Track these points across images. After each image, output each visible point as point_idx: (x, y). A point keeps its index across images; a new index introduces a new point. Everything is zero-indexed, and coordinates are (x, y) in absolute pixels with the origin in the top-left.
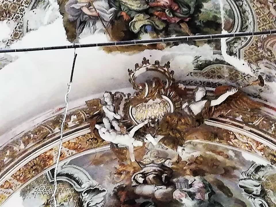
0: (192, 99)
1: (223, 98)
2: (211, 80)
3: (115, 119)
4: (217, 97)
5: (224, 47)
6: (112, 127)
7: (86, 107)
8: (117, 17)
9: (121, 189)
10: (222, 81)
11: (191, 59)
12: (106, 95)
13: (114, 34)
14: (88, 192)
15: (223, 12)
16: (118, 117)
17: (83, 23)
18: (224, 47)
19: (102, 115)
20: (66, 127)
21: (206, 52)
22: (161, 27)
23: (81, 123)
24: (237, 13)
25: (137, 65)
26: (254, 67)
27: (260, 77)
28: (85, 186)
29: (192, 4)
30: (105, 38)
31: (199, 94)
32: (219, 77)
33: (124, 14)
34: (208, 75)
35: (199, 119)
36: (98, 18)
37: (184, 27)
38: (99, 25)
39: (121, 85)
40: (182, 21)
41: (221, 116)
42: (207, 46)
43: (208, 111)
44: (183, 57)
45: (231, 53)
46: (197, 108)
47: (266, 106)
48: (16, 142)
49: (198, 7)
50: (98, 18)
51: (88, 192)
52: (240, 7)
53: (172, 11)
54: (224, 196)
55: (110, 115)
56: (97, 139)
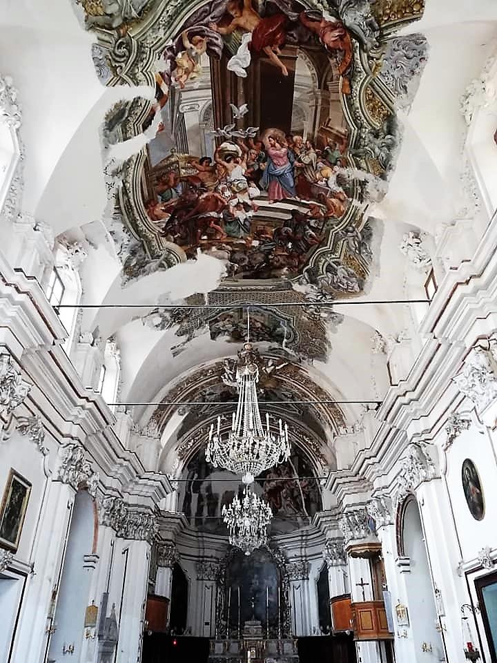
0: (267, 365)
1: (282, 366)
5: (284, 345)
7: (215, 365)
8: (235, 330)
11: (267, 346)
13: (233, 337)
14: (208, 395)
15: (285, 333)
17: (220, 333)
18: (284, 345)
19: (224, 371)
20: (206, 375)
21: (275, 345)
24: (292, 334)
28: (207, 392)
29: (272, 328)
30: (228, 338)
34: (274, 353)
37: (267, 336)
38: (226, 333)
39: (230, 354)
41: (281, 373)
43: (274, 371)
44: (264, 346)
45: (286, 347)
46: (269, 370)
49: (275, 329)
50: (225, 331)
51: (208, 395)
53: (263, 330)
54: (272, 395)
55: (229, 372)
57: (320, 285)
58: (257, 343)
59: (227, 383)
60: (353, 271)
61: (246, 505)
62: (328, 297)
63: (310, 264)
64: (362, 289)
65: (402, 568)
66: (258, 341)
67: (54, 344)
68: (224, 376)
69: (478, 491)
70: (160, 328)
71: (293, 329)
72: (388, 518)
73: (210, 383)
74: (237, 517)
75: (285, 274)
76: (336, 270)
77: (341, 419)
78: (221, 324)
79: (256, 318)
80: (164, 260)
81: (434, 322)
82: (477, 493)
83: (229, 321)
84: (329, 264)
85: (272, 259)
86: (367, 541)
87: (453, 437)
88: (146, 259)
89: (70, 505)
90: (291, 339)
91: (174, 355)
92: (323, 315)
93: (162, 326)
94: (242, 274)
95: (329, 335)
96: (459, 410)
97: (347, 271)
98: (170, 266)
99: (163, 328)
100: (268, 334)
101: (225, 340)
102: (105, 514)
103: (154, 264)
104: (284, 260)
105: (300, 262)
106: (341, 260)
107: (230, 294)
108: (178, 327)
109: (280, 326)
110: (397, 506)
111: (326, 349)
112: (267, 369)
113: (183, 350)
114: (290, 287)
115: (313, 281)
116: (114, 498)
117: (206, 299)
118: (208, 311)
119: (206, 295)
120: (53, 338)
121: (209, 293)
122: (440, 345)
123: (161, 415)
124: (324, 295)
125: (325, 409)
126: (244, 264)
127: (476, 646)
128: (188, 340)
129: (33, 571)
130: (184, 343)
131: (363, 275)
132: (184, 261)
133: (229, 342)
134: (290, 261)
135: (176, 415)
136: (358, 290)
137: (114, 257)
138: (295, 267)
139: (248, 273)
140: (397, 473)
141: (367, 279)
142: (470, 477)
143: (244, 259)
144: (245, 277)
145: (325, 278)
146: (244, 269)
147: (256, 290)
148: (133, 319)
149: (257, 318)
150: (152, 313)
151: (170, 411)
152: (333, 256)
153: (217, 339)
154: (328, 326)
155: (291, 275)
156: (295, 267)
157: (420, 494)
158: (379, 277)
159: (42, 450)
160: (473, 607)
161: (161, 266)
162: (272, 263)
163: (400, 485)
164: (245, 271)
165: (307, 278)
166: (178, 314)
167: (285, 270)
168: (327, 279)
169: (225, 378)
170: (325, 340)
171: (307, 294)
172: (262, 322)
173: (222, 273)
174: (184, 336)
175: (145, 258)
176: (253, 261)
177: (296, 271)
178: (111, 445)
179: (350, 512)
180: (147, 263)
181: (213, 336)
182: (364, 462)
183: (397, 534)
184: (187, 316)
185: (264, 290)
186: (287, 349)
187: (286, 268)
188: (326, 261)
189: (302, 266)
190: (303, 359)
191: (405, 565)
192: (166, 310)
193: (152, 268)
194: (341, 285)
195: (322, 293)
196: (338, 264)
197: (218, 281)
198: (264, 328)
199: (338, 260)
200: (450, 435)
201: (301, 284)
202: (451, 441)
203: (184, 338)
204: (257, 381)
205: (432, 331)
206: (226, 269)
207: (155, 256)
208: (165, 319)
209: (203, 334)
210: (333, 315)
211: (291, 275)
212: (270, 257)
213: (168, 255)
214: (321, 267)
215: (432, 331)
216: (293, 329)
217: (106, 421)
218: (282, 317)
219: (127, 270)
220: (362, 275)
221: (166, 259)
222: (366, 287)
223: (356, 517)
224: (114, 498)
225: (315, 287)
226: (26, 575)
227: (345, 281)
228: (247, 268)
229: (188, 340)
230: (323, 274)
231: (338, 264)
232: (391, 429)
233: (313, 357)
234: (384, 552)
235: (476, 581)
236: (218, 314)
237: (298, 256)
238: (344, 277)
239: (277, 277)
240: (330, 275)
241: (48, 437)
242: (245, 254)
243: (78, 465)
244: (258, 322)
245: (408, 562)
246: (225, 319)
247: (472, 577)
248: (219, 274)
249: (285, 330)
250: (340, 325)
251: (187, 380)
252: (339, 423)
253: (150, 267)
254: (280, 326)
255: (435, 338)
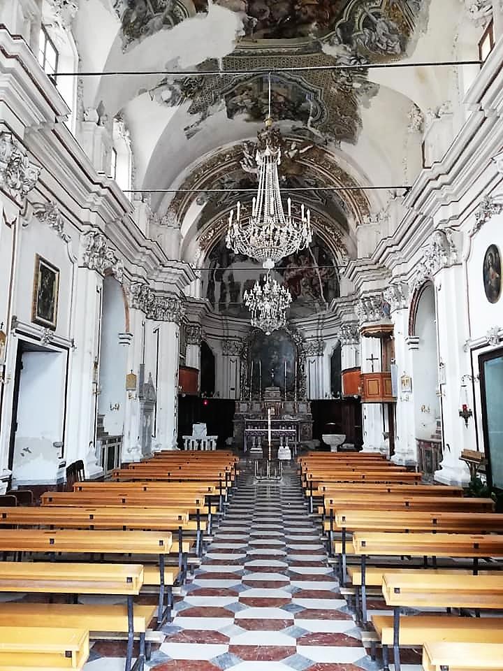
2: (299, 136)
3: (250, 159)
4: (302, 149)
5: (309, 124)
6: (248, 162)
7: (233, 149)
9: (243, 180)
10: (304, 137)
12: (245, 144)
15: (312, 108)
16: (252, 157)
17: (237, 110)
18: (309, 124)
19: (243, 156)
20: (224, 160)
21: (299, 124)
22: (277, 111)
23: (231, 158)
24: (319, 108)
25: (263, 130)
26: (323, 134)
27: (326, 141)
28: (226, 180)
30: (246, 116)
31: (293, 146)
32: (304, 135)
33: (259, 105)
35: (293, 160)
36: (245, 107)
37: (290, 113)
38: (245, 110)
40: (289, 110)
42: (300, 122)
43: (298, 155)
44: (286, 125)
45: (312, 126)
46: (291, 154)
47: (326, 152)
48: (199, 170)
49: (299, 104)
50: (243, 107)
51: (227, 183)
52: (321, 108)
53: (285, 105)
54: (294, 183)
55: (248, 156)
56: (240, 167)
57: (355, 45)
58: (278, 122)
59: (246, 169)
60: (395, 25)
61: (266, 290)
62: (363, 61)
63: (344, 16)
64: (403, 49)
65: (411, 346)
66: (279, 119)
67: (56, 122)
68: (243, 161)
69: (498, 276)
70: (170, 104)
71: (320, 104)
72: (403, 302)
73: (228, 170)
74: (258, 301)
75: (313, 31)
76: (374, 25)
77: (365, 207)
78: (238, 98)
79: (278, 91)
80: (169, 14)
81: (483, 90)
82: (497, 278)
83: (247, 95)
84: (367, 17)
85: (299, 10)
86: (381, 323)
87: (482, 222)
88: (148, 14)
89: (99, 289)
90: (318, 117)
91: (189, 136)
92: (356, 85)
93: (172, 102)
94: (263, 32)
95: (362, 111)
96: (493, 194)
97: (387, 25)
98: (176, 22)
99: (173, 105)
100: (293, 111)
101: (242, 119)
102: (134, 299)
103: (157, 20)
104: (314, 12)
105: (332, 14)
106: (382, 11)
107: (248, 59)
108: (189, 103)
109: (305, 101)
110: (414, 291)
111: (356, 128)
112: (290, 153)
113: (196, 131)
114: (319, 50)
115: (347, 41)
116: (140, 284)
117: (221, 67)
118: (224, 80)
119: (220, 62)
120: (54, 114)
121: (224, 58)
122: (485, 118)
123: (179, 204)
124: (359, 59)
125: (350, 197)
126: (264, 17)
127: (470, 407)
128: (203, 119)
129: (73, 346)
130: (198, 123)
131: (408, 31)
132: (193, 16)
133: (247, 121)
134: (320, 12)
135: (194, 203)
136: (399, 52)
137: (109, 10)
138: (327, 21)
139: (269, 31)
140: (417, 260)
141: (411, 34)
142: (492, 263)
143: (265, 11)
144: (266, 36)
145: (362, 36)
146: (264, 25)
147: (280, 53)
148: (139, 94)
149: (280, 90)
150: (162, 85)
151: (188, 200)
152: (374, 5)
153: (235, 117)
154: (360, 99)
155: (321, 33)
156: (327, 21)
157: (438, 281)
158: (425, 33)
159: (63, 237)
160: (473, 376)
161: (166, 22)
162: (299, 17)
163: (419, 271)
164: (265, 27)
165: (339, 36)
166: (190, 86)
167: (313, 26)
168: (363, 37)
169: (244, 164)
170: (356, 117)
171: (340, 57)
172: (285, 95)
173: (238, 32)
174: (198, 113)
175: (146, 12)
176: (276, 15)
177: (326, 26)
178: (131, 234)
179: (366, 298)
180: (150, 18)
181: (230, 115)
182: (385, 251)
183: (410, 316)
184: (200, 89)
185: (287, 53)
186: (313, 130)
187: (315, 23)
188: (365, 11)
189: (333, 20)
190: (330, 140)
191: (414, 343)
192: (176, 81)
193: (155, 25)
194: (380, 45)
195: (356, 55)
196: (378, 15)
197: (233, 41)
198: (287, 103)
199: (378, 10)
200: (479, 220)
201: (332, 44)
202: (479, 227)
203: (198, 116)
204: (279, 163)
205: (479, 102)
206: (243, 26)
207: (159, 9)
208: (174, 93)
209: (218, 112)
210: (367, 86)
211: (321, 33)
212: (297, 7)
213: (174, 7)
214: (357, 20)
215: (479, 102)
216: (320, 104)
217: (124, 210)
218: (308, 89)
219: (127, 29)
220: (405, 30)
221: (172, 13)
222: (409, 48)
223: (372, 302)
224: (140, 284)
225: (348, 48)
226: (68, 349)
227: (384, 40)
228: (268, 23)
229: (203, 119)
230: (359, 31)
231: (378, 15)
232: (417, 216)
233: (340, 138)
234: (395, 332)
235: (480, 356)
236: (235, 85)
237: (330, 6)
238: (384, 34)
239: (302, 35)
240: (367, 31)
241: (67, 225)
242: (266, 4)
243: (102, 252)
244: (280, 95)
245: (417, 340)
246: (243, 92)
247: (476, 353)
248: (235, 33)
249: (312, 105)
250: (375, 97)
251: (203, 166)
252: (363, 212)
253: (153, 24)
254: (305, 101)
255: (481, 110)
